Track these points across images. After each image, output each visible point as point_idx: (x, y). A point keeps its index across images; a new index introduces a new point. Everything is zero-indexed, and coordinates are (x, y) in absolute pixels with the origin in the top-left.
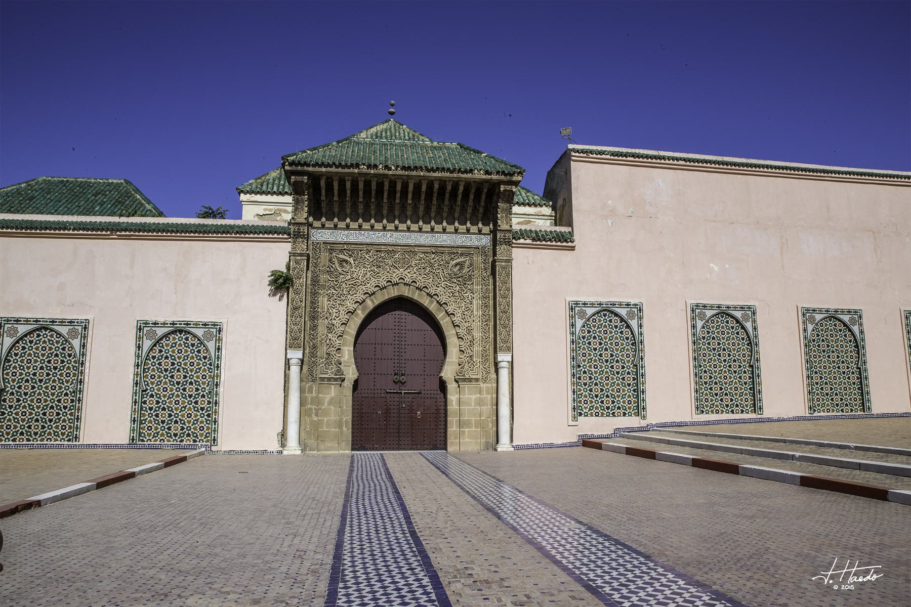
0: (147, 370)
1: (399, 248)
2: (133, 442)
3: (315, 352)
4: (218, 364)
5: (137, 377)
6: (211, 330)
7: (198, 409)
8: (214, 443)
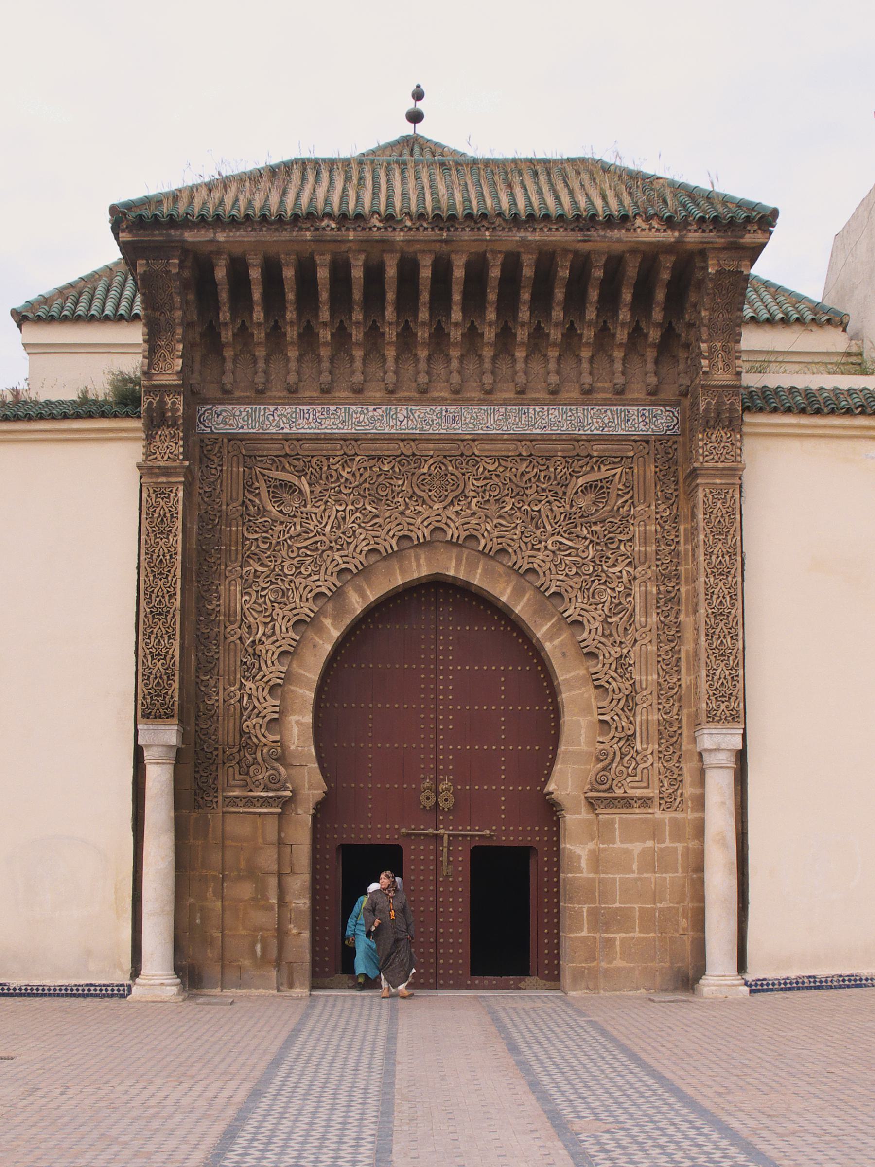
1: (431, 446)
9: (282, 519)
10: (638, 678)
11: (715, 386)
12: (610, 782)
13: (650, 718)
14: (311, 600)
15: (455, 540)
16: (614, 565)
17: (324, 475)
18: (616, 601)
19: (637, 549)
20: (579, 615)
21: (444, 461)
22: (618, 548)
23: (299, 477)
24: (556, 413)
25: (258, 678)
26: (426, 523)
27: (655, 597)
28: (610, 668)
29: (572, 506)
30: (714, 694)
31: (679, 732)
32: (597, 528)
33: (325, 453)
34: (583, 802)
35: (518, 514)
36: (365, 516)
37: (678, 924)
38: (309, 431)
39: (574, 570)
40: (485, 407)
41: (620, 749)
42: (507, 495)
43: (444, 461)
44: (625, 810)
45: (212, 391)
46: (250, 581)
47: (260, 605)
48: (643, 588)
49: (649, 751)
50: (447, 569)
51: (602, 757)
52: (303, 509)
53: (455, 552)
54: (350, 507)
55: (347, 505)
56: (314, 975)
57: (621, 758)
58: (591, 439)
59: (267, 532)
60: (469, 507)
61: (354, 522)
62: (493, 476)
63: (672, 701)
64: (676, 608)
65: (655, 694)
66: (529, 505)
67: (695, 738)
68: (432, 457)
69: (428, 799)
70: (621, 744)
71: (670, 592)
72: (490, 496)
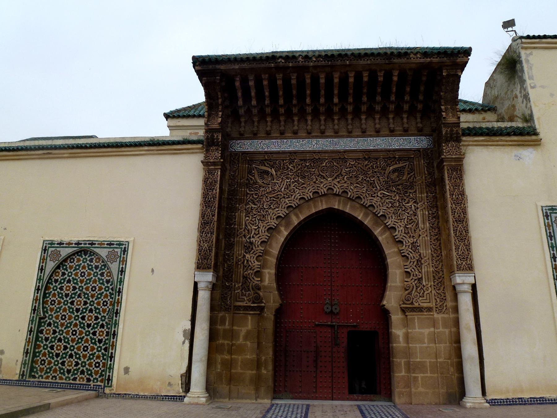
0: (48, 295)
1: (327, 155)
2: (22, 377)
3: (230, 275)
4: (120, 288)
5: (36, 303)
6: (116, 250)
7: (95, 341)
8: (108, 384)
9: (264, 186)
10: (422, 252)
11: (449, 123)
12: (412, 300)
13: (429, 270)
14: (275, 219)
15: (337, 193)
16: (408, 203)
17: (281, 168)
18: (410, 218)
19: (418, 195)
20: (394, 224)
21: (333, 161)
22: (409, 195)
23: (271, 169)
24: (379, 140)
25: (251, 252)
26: (325, 186)
27: (427, 216)
28: (409, 248)
29: (388, 178)
30: (459, 257)
31: (443, 276)
32: (400, 187)
33: (282, 158)
34: (399, 310)
35: (365, 182)
36: (299, 184)
37: (448, 370)
38: (275, 150)
39: (390, 205)
40: (349, 139)
41: (416, 284)
42: (360, 174)
43: (333, 161)
44: (420, 313)
45: (235, 134)
46: (249, 211)
47: (253, 221)
48: (422, 212)
49: (429, 285)
50: (335, 206)
51: (407, 288)
52: (272, 181)
53: (338, 198)
54: (292, 181)
55: (291, 180)
56: (275, 392)
57: (416, 289)
58: (395, 150)
59: (257, 191)
60: (344, 180)
61: (294, 186)
62: (354, 167)
63: (438, 262)
64: (437, 221)
65: (430, 259)
66: (369, 178)
67: (451, 279)
68: (327, 159)
69: (328, 308)
70: (416, 282)
71: (434, 214)
72: (352, 175)
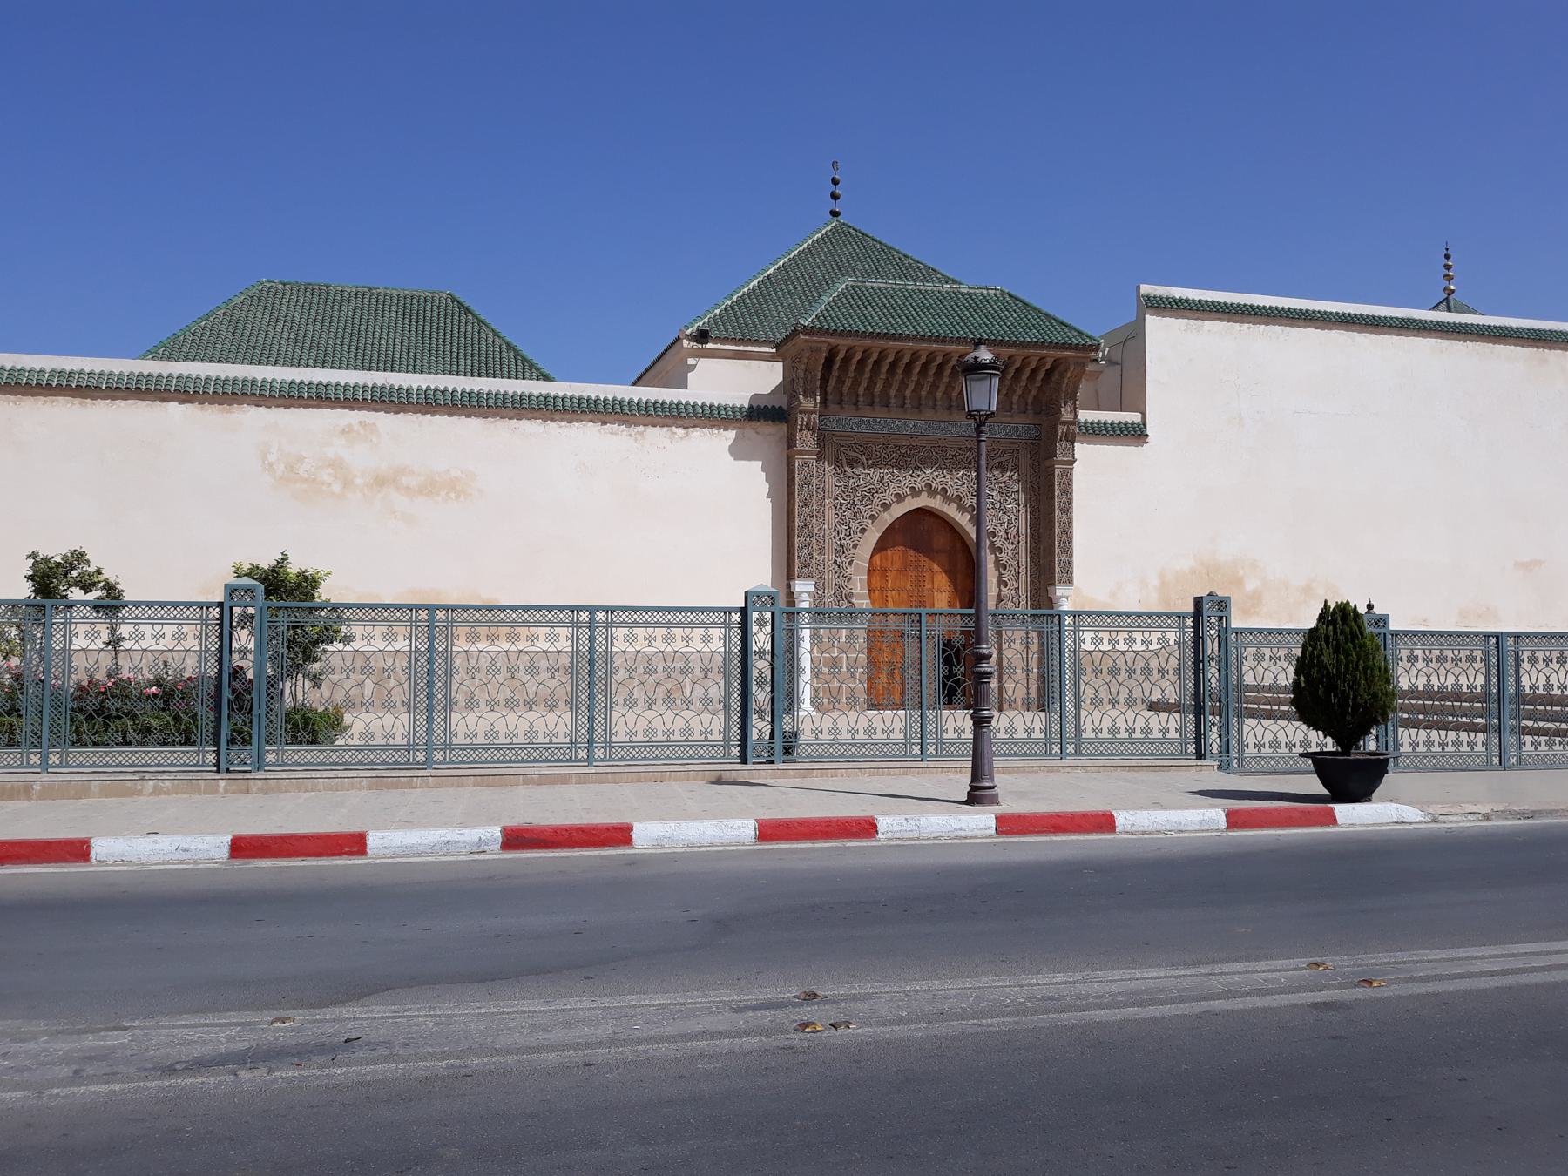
60: (943, 473)
